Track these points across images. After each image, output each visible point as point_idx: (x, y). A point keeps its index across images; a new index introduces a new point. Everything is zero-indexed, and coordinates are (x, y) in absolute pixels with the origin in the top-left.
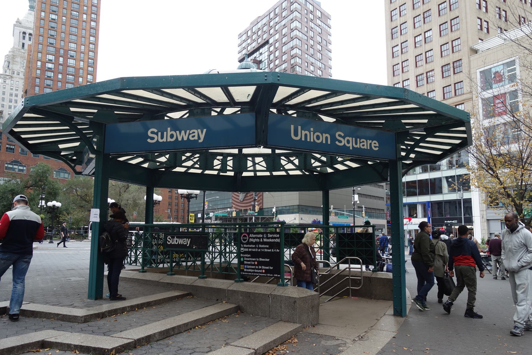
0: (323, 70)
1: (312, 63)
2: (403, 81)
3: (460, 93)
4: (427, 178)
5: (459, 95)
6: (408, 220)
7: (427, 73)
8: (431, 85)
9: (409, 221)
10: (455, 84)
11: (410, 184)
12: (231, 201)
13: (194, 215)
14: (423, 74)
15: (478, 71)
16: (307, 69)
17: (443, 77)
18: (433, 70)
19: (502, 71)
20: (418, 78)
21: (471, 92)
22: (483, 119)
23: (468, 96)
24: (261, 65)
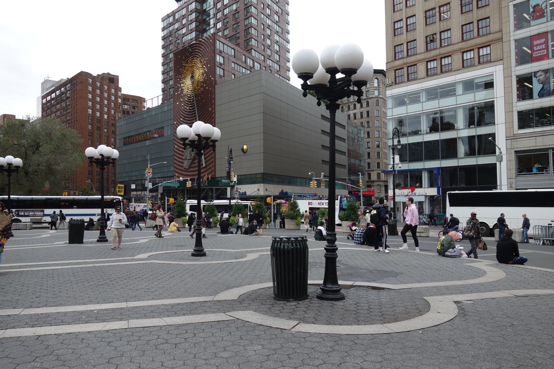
0: (281, 16)
1: (269, 5)
2: (407, 18)
3: (484, 33)
4: (438, 138)
5: (483, 35)
6: (410, 190)
7: (440, 7)
8: (445, 23)
9: (412, 192)
10: (478, 21)
11: (413, 146)
12: (172, 169)
13: (123, 186)
14: (434, 8)
15: (511, 4)
16: (263, 11)
17: (462, 13)
18: (449, 3)
19: (545, 4)
20: (428, 13)
21: (501, 31)
22: (516, 66)
23: (498, 35)
24: (205, 5)
